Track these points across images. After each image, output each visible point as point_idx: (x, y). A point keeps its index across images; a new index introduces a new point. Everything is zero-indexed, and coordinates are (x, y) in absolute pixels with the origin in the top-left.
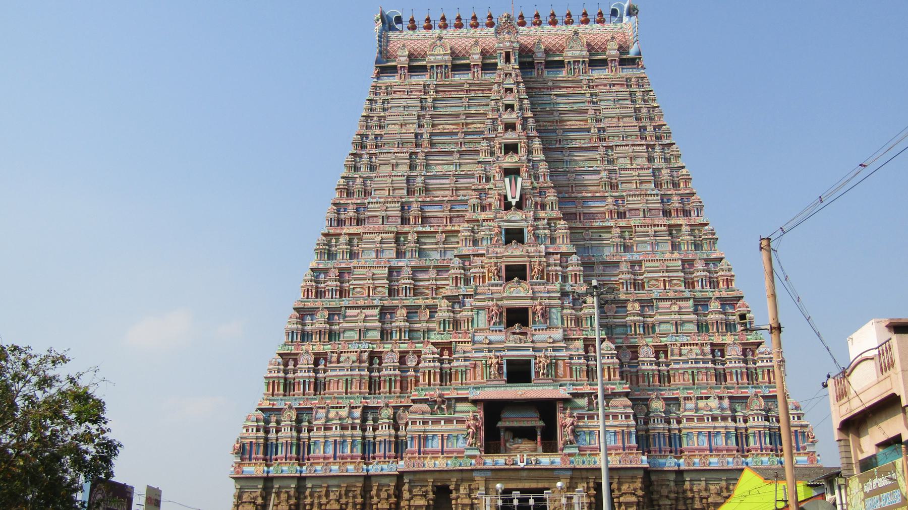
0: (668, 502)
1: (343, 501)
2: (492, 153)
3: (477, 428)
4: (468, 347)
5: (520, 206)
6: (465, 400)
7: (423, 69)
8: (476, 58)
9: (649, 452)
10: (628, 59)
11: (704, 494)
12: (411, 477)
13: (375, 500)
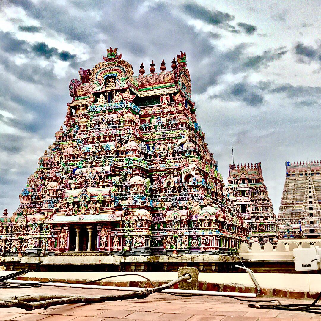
7: (294, 175)
8: (304, 172)
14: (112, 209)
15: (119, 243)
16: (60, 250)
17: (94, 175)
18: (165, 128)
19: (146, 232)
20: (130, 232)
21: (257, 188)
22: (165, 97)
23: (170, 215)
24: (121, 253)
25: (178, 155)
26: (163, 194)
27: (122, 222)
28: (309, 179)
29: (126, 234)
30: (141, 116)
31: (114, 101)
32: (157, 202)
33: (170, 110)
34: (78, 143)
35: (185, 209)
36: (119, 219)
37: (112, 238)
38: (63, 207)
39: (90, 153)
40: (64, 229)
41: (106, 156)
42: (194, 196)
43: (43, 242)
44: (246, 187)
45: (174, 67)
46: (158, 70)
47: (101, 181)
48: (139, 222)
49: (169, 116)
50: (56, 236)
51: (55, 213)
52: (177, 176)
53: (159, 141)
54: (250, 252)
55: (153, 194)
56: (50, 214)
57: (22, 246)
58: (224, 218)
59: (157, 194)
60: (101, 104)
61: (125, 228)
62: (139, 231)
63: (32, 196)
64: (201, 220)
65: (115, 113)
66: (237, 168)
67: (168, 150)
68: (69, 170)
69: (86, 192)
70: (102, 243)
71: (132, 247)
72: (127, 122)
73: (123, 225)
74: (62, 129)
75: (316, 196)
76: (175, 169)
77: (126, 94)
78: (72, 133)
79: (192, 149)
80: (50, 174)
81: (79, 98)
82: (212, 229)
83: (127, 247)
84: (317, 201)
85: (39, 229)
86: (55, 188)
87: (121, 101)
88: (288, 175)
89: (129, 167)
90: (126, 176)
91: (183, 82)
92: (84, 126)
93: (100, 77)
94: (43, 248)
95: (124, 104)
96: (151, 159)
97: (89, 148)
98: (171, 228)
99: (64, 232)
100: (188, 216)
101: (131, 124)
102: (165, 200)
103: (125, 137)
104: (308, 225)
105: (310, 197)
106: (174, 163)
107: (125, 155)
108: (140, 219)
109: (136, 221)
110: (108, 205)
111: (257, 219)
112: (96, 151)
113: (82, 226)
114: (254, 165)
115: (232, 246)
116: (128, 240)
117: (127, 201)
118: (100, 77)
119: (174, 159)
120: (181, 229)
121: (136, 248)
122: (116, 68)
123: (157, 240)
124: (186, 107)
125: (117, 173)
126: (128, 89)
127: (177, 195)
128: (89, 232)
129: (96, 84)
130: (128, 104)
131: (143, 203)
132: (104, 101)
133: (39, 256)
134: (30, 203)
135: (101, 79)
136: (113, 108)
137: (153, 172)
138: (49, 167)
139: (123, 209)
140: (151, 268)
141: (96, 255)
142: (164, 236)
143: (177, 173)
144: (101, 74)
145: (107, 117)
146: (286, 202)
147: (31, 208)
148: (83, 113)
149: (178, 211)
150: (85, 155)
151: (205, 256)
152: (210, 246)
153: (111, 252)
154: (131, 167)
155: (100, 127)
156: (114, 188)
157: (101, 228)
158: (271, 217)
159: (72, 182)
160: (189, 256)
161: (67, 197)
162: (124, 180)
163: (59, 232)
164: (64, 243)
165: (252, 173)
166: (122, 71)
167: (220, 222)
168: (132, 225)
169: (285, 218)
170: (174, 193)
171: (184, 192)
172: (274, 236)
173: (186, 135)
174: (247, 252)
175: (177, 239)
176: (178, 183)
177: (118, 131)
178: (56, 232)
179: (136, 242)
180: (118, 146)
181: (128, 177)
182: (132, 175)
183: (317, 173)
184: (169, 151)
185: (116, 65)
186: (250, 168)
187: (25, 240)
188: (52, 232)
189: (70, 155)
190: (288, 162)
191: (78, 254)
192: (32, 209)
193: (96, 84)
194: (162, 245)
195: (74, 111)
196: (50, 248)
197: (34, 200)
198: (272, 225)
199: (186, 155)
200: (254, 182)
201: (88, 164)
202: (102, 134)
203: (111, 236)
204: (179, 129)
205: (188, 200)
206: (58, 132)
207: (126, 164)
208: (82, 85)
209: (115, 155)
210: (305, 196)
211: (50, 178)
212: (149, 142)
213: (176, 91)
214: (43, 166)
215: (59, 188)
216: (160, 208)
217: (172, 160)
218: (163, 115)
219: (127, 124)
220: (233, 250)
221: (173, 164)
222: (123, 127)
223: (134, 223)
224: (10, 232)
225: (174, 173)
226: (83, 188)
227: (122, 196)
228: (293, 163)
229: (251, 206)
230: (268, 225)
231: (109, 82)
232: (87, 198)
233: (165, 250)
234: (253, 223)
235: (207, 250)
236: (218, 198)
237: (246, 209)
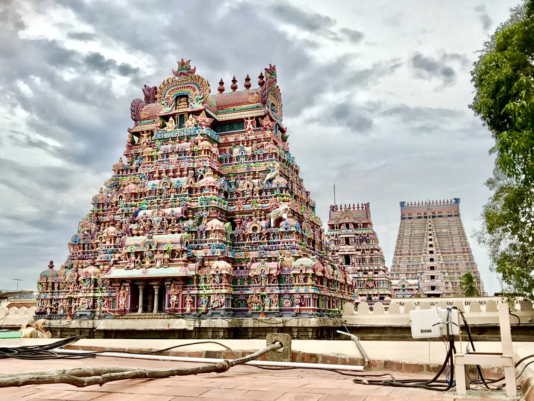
7: (411, 218)
8: (423, 215)
14: (184, 261)
15: (193, 303)
16: (118, 312)
17: (162, 218)
18: (250, 159)
19: (227, 289)
20: (206, 289)
21: (365, 234)
22: (249, 121)
23: (256, 268)
24: (195, 316)
25: (266, 194)
26: (247, 242)
27: (196, 277)
28: (430, 224)
29: (201, 292)
30: (220, 145)
31: (187, 126)
32: (239, 252)
33: (256, 137)
34: (141, 179)
35: (275, 261)
36: (193, 273)
37: (184, 297)
38: (122, 258)
39: (156, 190)
40: (125, 286)
41: (176, 194)
42: (285, 244)
43: (98, 301)
44: (351, 233)
45: (261, 84)
46: (241, 87)
47: (170, 225)
48: (217, 277)
49: (254, 145)
50: (114, 294)
51: (112, 266)
52: (265, 219)
53: (242, 177)
54: (356, 315)
55: (235, 242)
56: (106, 267)
57: (72, 307)
58: (323, 272)
59: (239, 242)
60: (170, 130)
61: (199, 285)
62: (218, 289)
63: (84, 245)
64: (295, 275)
65: (187, 142)
66: (339, 210)
67: (254, 187)
68: (130, 212)
69: (151, 240)
70: (171, 303)
71: (208, 308)
72: (203, 152)
73: (198, 281)
74: (122, 161)
75: (437, 244)
76: (262, 210)
77: (202, 117)
78: (134, 166)
79: (284, 186)
80: (107, 218)
81: (142, 122)
82: (308, 285)
83: (203, 308)
84: (439, 251)
85: (92, 286)
86: (113, 234)
87: (196, 126)
88: (403, 218)
89: (204, 208)
90: (201, 219)
91: (272, 102)
92: (149, 156)
93: (168, 95)
94: (98, 309)
95: (198, 130)
96: (233, 198)
97: (155, 185)
98: (257, 285)
99: (124, 289)
100: (278, 269)
101: (208, 154)
102: (250, 249)
103: (200, 170)
104: (429, 281)
105: (431, 246)
106: (262, 203)
107: (200, 193)
108: (219, 273)
109: (214, 275)
110: (178, 255)
111: (365, 274)
112: (164, 188)
113: (147, 282)
114: (360, 206)
115: (333, 307)
116: (203, 299)
117: (203, 251)
118: (168, 95)
119: (261, 198)
120: (269, 286)
121: (214, 309)
122: (188, 85)
123: (239, 300)
124: (276, 133)
125: (190, 216)
126: (204, 111)
127: (265, 243)
128: (155, 290)
129: (164, 105)
130: (204, 130)
131: (222, 253)
132: (174, 126)
133: (93, 319)
134: (81, 254)
135: (170, 98)
136: (185, 135)
137: (235, 215)
138: (105, 208)
139: (197, 261)
140: (232, 335)
141: (163, 318)
142: (249, 294)
143: (265, 215)
144: (170, 92)
145: (178, 146)
146: (401, 252)
147: (83, 259)
148: (147, 140)
149: (266, 263)
150: (150, 193)
151: (300, 320)
152: (306, 307)
153: (182, 315)
154: (207, 209)
155: (169, 158)
156: (186, 234)
157: (170, 285)
158: (381, 271)
159: (134, 226)
160: (279, 320)
161: (127, 246)
162: (198, 225)
163: (118, 290)
164: (123, 303)
165: (358, 216)
166: (196, 88)
167: (318, 277)
168: (208, 281)
170: (261, 241)
171: (274, 239)
172: (386, 295)
173: (276, 168)
174: (353, 314)
175: (265, 297)
176: (267, 228)
177: (191, 163)
178: (114, 289)
179: (213, 302)
180: (191, 183)
181: (204, 221)
182: (209, 218)
183: (439, 216)
184: (255, 189)
185: (189, 81)
186: (356, 209)
187: (75, 299)
188: (109, 290)
189: (132, 194)
190: (404, 203)
191: (141, 317)
192: (85, 261)
193: (164, 105)
194: (246, 305)
195: (136, 139)
196: (107, 309)
197: (86, 250)
198: (383, 280)
199: (275, 194)
200: (360, 227)
201: (153, 204)
202: (172, 167)
203: (183, 295)
204: (267, 161)
205: (278, 249)
206: (117, 165)
207: (202, 205)
208: (146, 106)
209: (187, 193)
210: (424, 244)
211: (106, 222)
212: (230, 177)
213: (263, 114)
214: (98, 207)
215: (118, 234)
216: (243, 260)
217: (259, 199)
218: (248, 143)
219: (203, 155)
220: (335, 312)
221: (260, 205)
222: (198, 158)
223: (211, 278)
224: (56, 290)
225: (261, 216)
226: (147, 235)
227: (196, 245)
228: (410, 203)
229: (358, 257)
230: (378, 281)
231: (180, 102)
232: (153, 247)
233: (250, 312)
234: (360, 278)
235: (303, 312)
236: (316, 246)
237: (351, 261)
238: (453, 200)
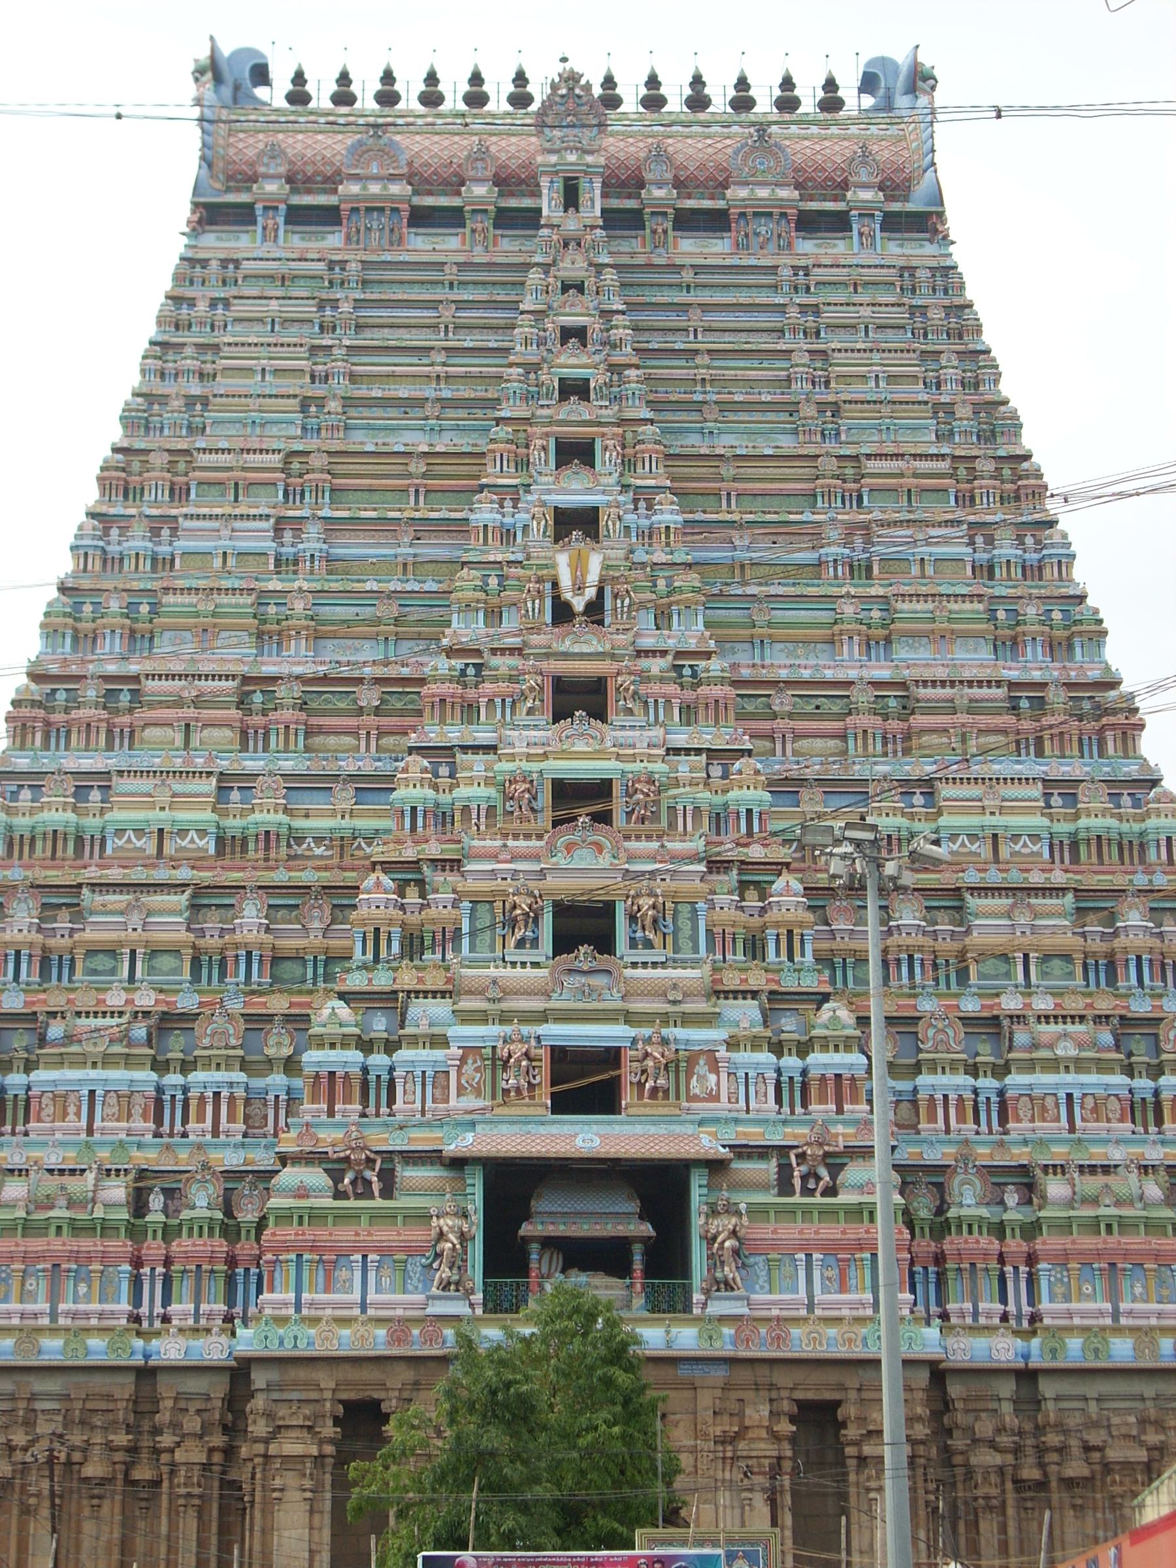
0: (997, 1459)
1: (77, 1438)
2: (523, 464)
3: (463, 1237)
4: (439, 1009)
5: (595, 609)
6: (432, 1157)
9: (944, 1316)
10: (909, 214)
11: (1095, 1437)
12: (273, 1375)
13: (166, 1440)
28: (573, 266)
169: (92, 873)
238: (848, 92)
